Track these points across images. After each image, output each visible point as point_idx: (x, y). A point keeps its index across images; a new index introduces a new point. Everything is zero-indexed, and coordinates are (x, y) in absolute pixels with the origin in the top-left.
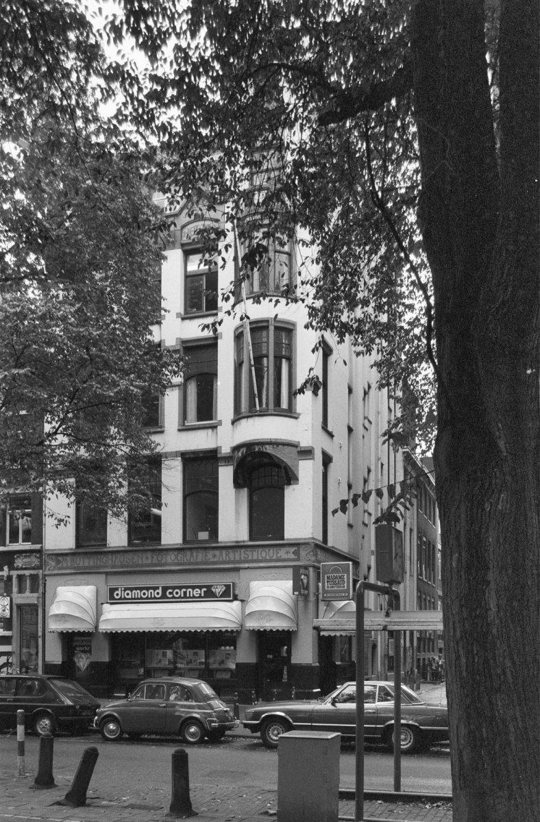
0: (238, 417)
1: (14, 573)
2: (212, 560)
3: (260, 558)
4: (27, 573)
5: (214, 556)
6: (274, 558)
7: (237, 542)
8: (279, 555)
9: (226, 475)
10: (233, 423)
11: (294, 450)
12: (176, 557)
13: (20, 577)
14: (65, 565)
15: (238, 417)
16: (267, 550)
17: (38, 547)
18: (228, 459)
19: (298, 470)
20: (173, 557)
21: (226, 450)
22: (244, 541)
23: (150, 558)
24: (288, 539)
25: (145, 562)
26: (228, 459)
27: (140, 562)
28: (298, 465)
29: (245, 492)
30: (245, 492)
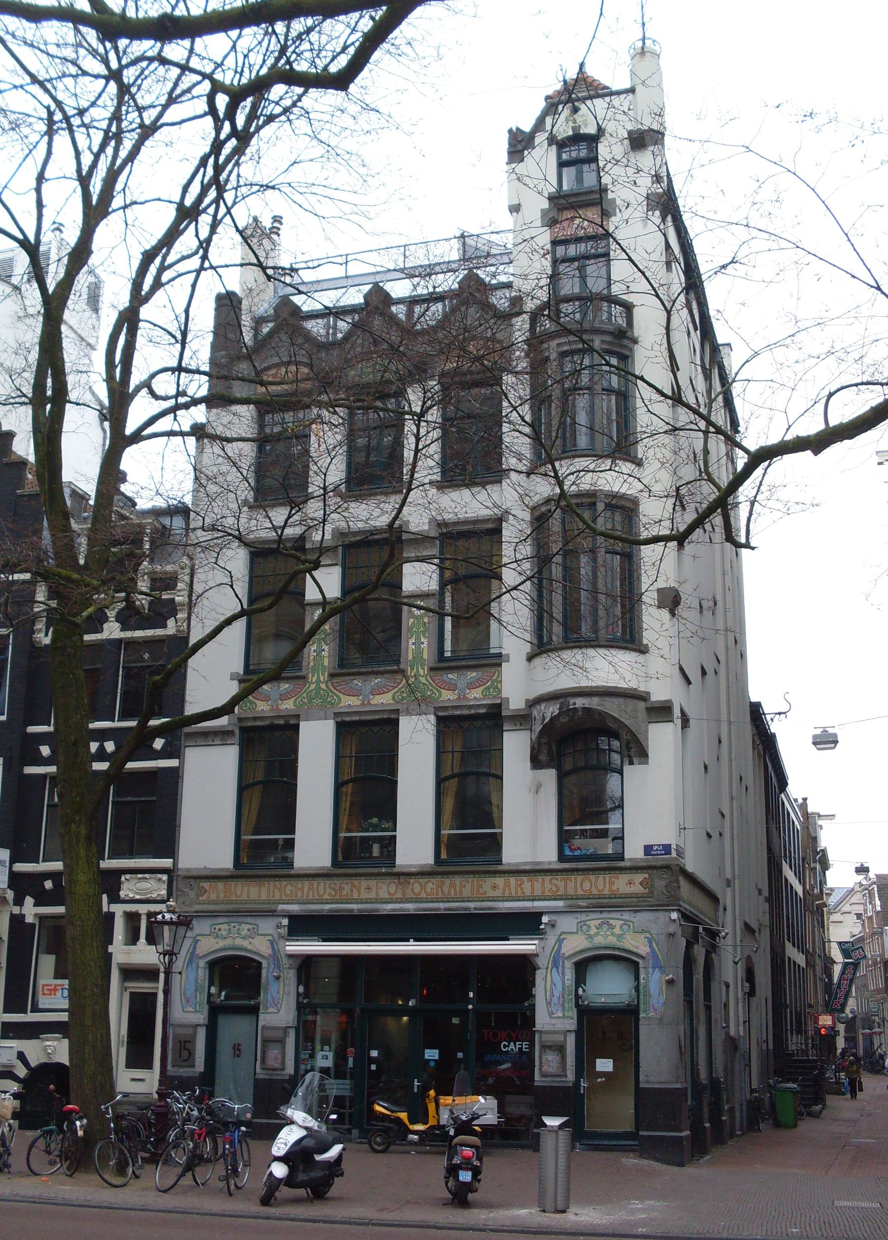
0: (542, 647)
1: (118, 910)
2: (491, 893)
3: (580, 892)
4: (143, 909)
5: (494, 887)
6: (606, 892)
7: (532, 863)
8: (614, 888)
9: (515, 747)
10: (530, 658)
11: (642, 705)
12: (423, 887)
13: (132, 919)
14: (213, 897)
15: (542, 647)
16: (593, 878)
17: (167, 863)
18: (523, 719)
19: (647, 739)
20: (417, 888)
21: (516, 702)
22: (550, 863)
23: (374, 889)
24: (631, 859)
25: (364, 895)
26: (523, 719)
27: (355, 896)
28: (646, 732)
29: (549, 776)
30: (549, 776)
